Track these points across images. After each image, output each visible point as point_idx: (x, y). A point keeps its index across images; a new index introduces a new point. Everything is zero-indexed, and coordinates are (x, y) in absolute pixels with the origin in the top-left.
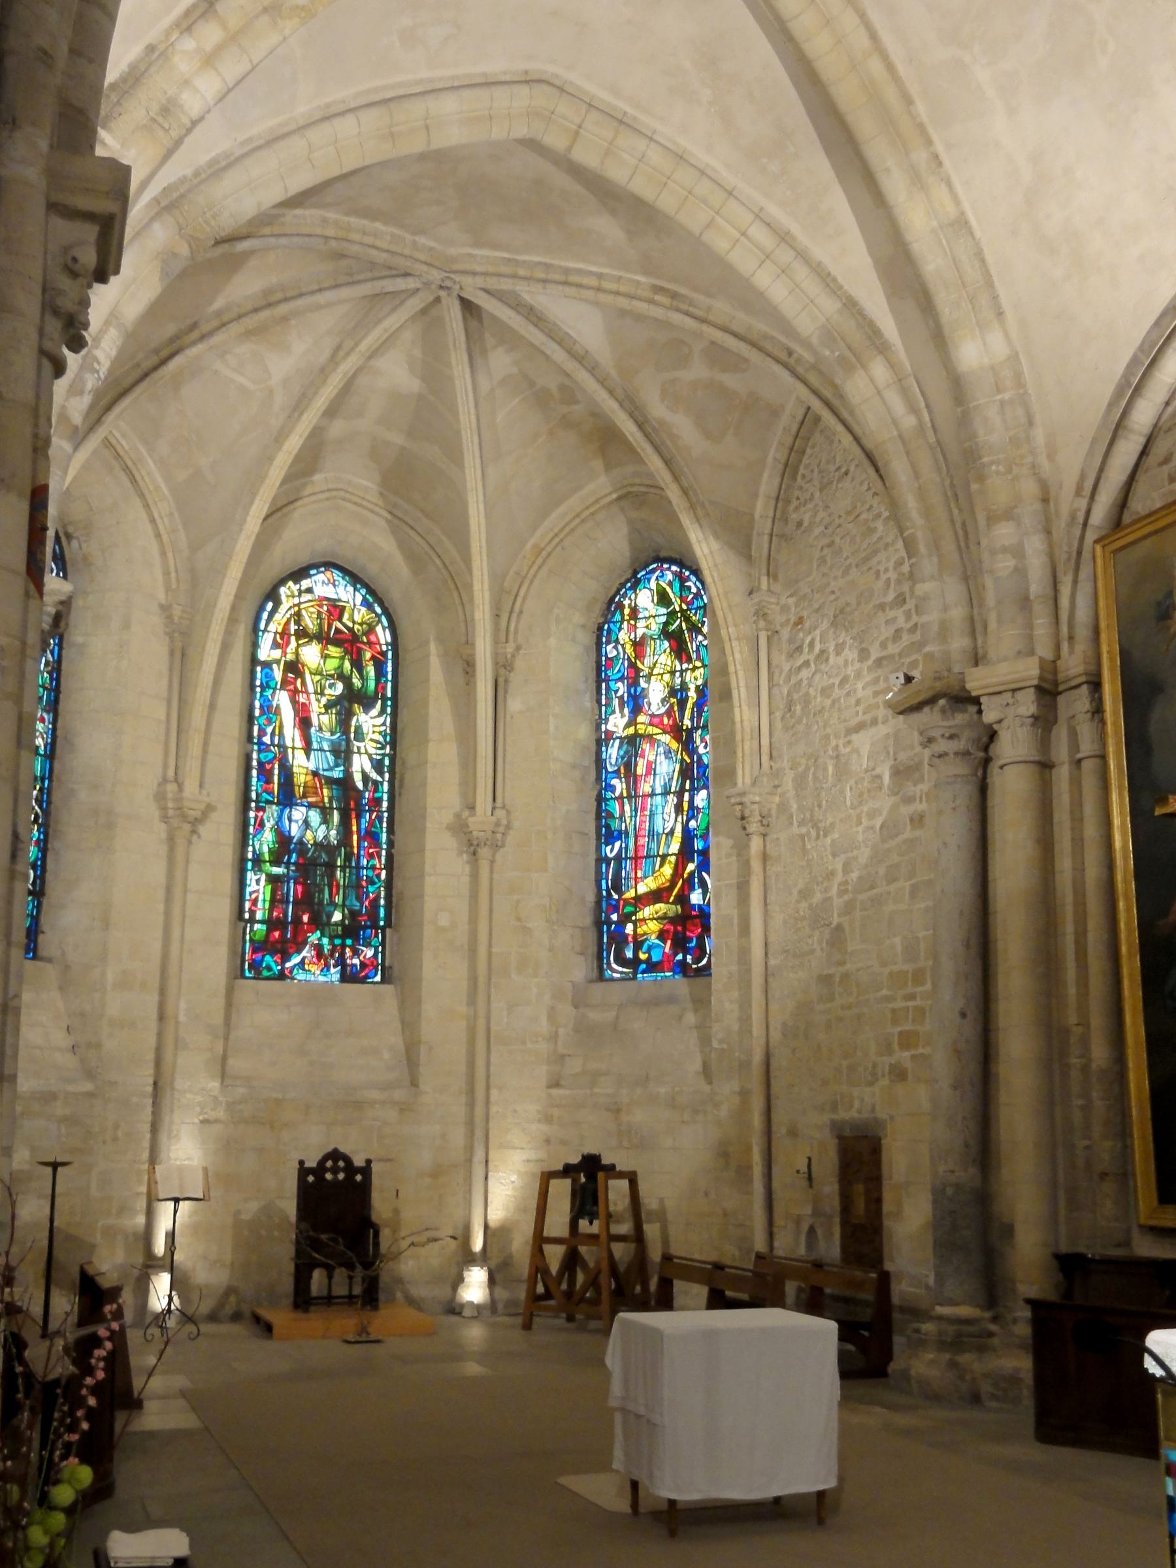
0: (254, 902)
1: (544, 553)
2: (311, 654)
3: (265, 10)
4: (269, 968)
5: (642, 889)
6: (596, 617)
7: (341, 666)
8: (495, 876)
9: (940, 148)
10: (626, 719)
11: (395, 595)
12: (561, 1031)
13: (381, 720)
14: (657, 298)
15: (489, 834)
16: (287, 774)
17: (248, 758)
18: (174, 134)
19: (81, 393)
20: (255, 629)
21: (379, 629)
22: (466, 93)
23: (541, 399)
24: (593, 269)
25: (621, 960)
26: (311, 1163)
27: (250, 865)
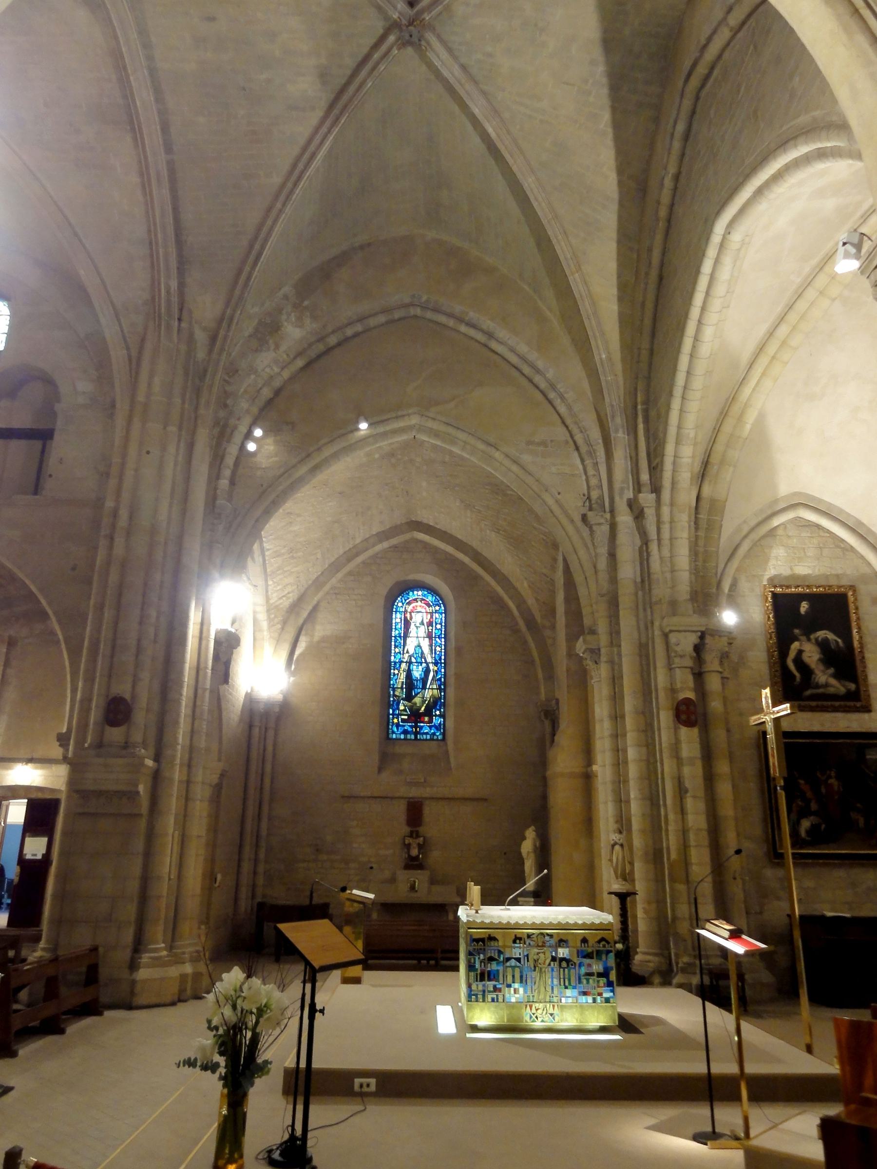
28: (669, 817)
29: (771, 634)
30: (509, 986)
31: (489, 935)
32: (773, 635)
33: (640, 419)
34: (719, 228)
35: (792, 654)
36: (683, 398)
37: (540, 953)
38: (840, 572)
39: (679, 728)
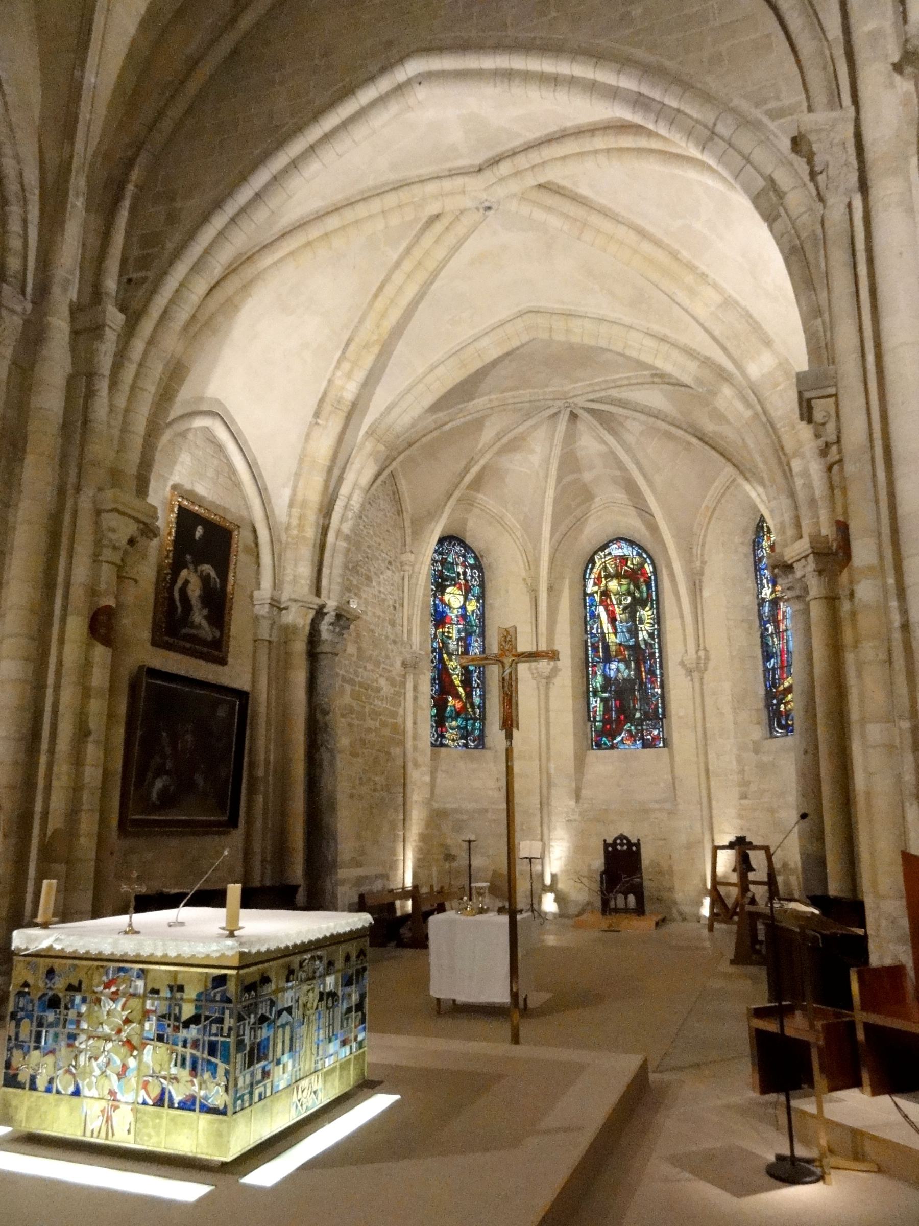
0: (595, 712)
1: (711, 510)
2: (613, 585)
3: (364, 347)
4: (605, 744)
5: (786, 684)
6: (751, 536)
7: (629, 588)
8: (705, 687)
9: (703, 268)
10: (770, 590)
11: (649, 546)
12: (747, 768)
13: (650, 613)
14: (656, 380)
15: (695, 665)
16: (606, 647)
17: (586, 642)
18: (346, 408)
19: (347, 521)
20: (584, 579)
21: (646, 566)
22: (491, 334)
23: (669, 436)
24: (627, 375)
25: (780, 726)
26: (610, 841)
27: (591, 694)
28: (56, 769)
29: (169, 551)
30: (278, 1062)
31: (263, 974)
32: (171, 554)
33: (127, 203)
34: (414, 67)
35: (180, 583)
36: (233, 220)
37: (308, 991)
38: (227, 506)
39: (94, 645)
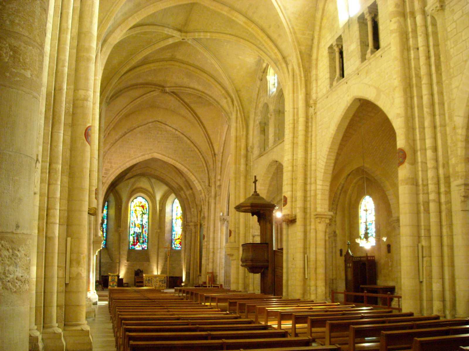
26: (136, 270)
